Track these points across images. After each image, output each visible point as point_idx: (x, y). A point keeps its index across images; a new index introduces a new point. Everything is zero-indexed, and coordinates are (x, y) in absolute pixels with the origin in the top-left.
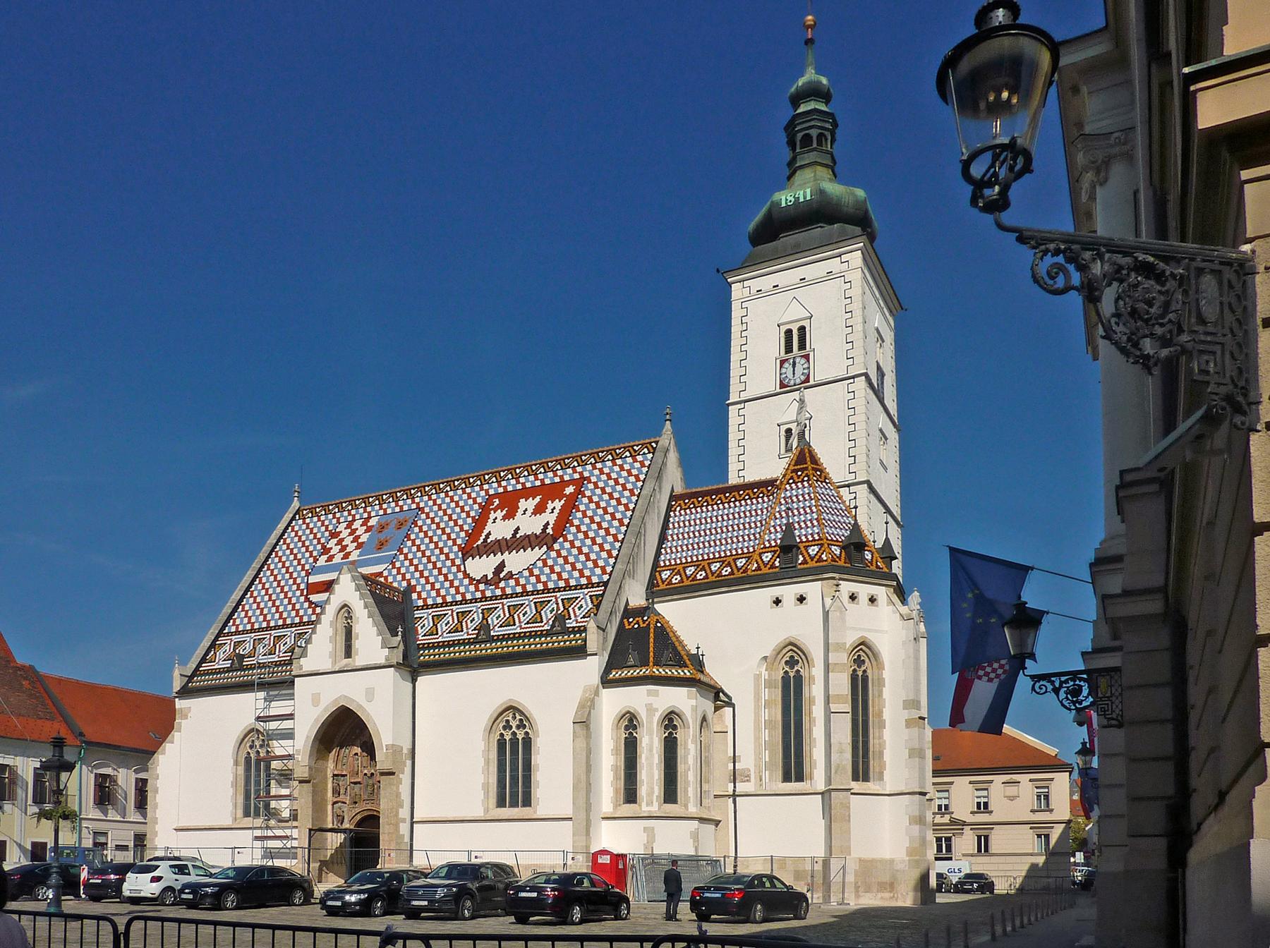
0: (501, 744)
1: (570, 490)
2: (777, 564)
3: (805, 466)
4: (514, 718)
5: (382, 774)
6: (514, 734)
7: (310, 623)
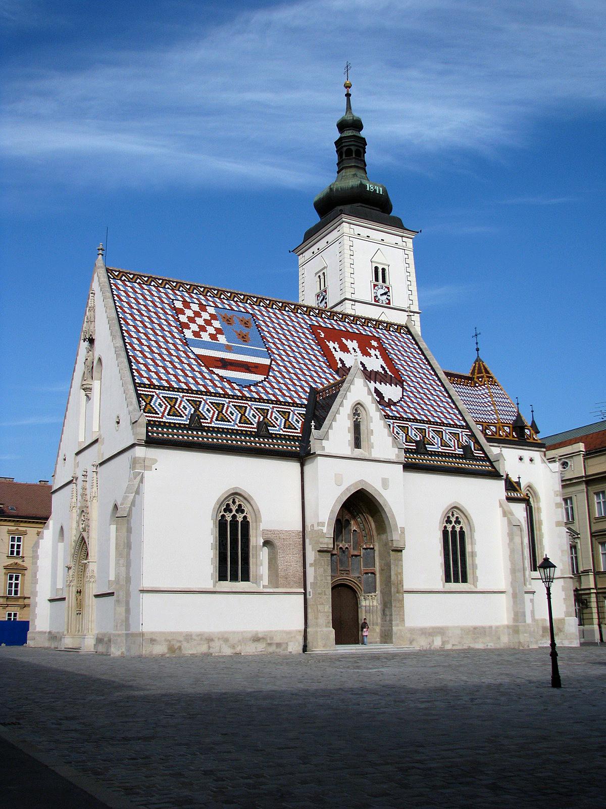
0: (445, 532)
1: (374, 343)
2: (516, 436)
3: (482, 375)
4: (453, 515)
5: (393, 550)
6: (453, 527)
7: (238, 397)
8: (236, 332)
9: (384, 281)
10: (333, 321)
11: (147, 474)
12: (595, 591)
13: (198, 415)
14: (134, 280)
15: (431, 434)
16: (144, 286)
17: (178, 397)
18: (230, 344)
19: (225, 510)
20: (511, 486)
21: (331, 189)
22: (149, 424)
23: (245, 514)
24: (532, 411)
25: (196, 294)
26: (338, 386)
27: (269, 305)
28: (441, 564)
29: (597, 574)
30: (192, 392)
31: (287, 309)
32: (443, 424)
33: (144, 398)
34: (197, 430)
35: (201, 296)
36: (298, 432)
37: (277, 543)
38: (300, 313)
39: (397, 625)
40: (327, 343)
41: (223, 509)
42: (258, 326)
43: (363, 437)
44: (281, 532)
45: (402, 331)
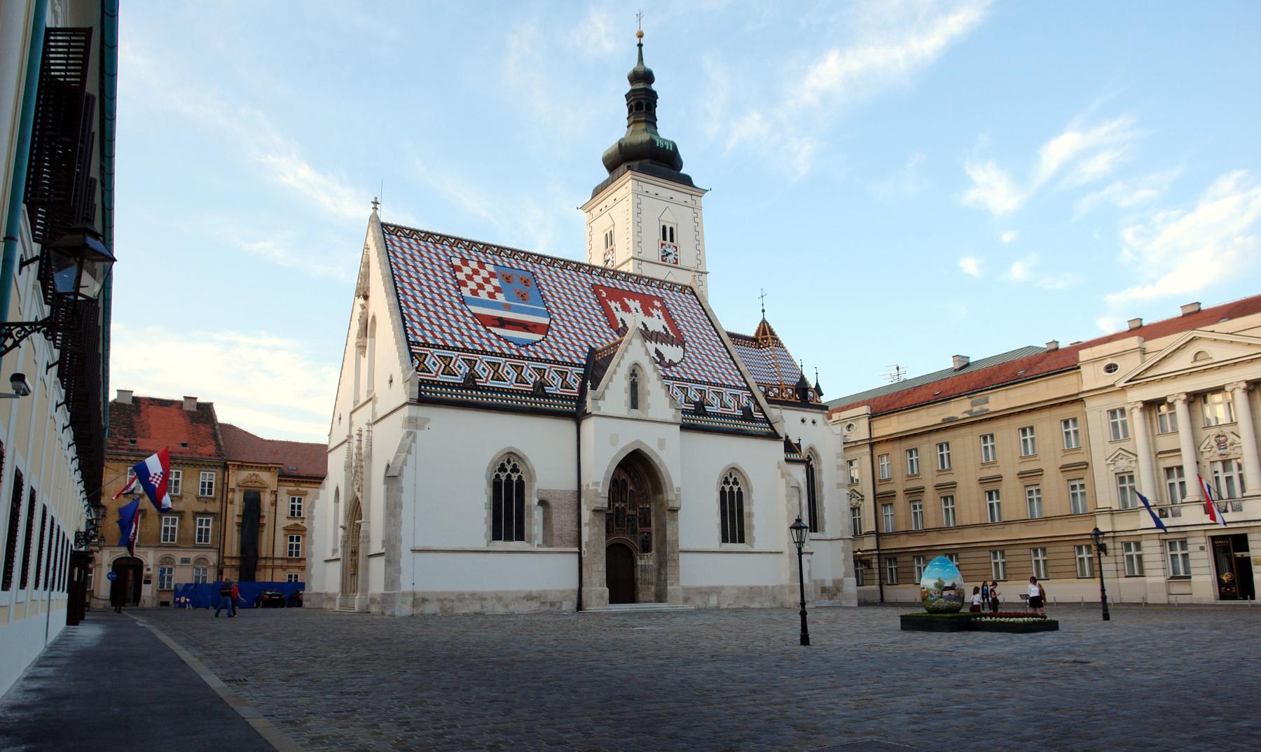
0: (723, 492)
1: (657, 304)
4: (731, 476)
5: (669, 510)
6: (731, 488)
7: (515, 357)
8: (516, 291)
9: (672, 240)
10: (615, 280)
11: (420, 433)
12: (877, 552)
13: (472, 375)
14: (410, 236)
15: (711, 395)
16: (421, 242)
17: (453, 356)
18: (508, 302)
19: (500, 470)
20: (790, 447)
21: (620, 144)
22: (422, 383)
23: (520, 474)
24: (817, 374)
25: (475, 251)
26: (615, 345)
27: (550, 263)
28: (718, 524)
29: (878, 535)
30: (468, 351)
31: (569, 267)
32: (723, 385)
33: (418, 357)
34: (472, 390)
35: (480, 254)
36: (575, 392)
37: (552, 502)
38: (583, 272)
39: (672, 584)
40: (609, 302)
41: (497, 468)
42: (538, 285)
43: (639, 397)
44: (556, 491)
45: (686, 291)
